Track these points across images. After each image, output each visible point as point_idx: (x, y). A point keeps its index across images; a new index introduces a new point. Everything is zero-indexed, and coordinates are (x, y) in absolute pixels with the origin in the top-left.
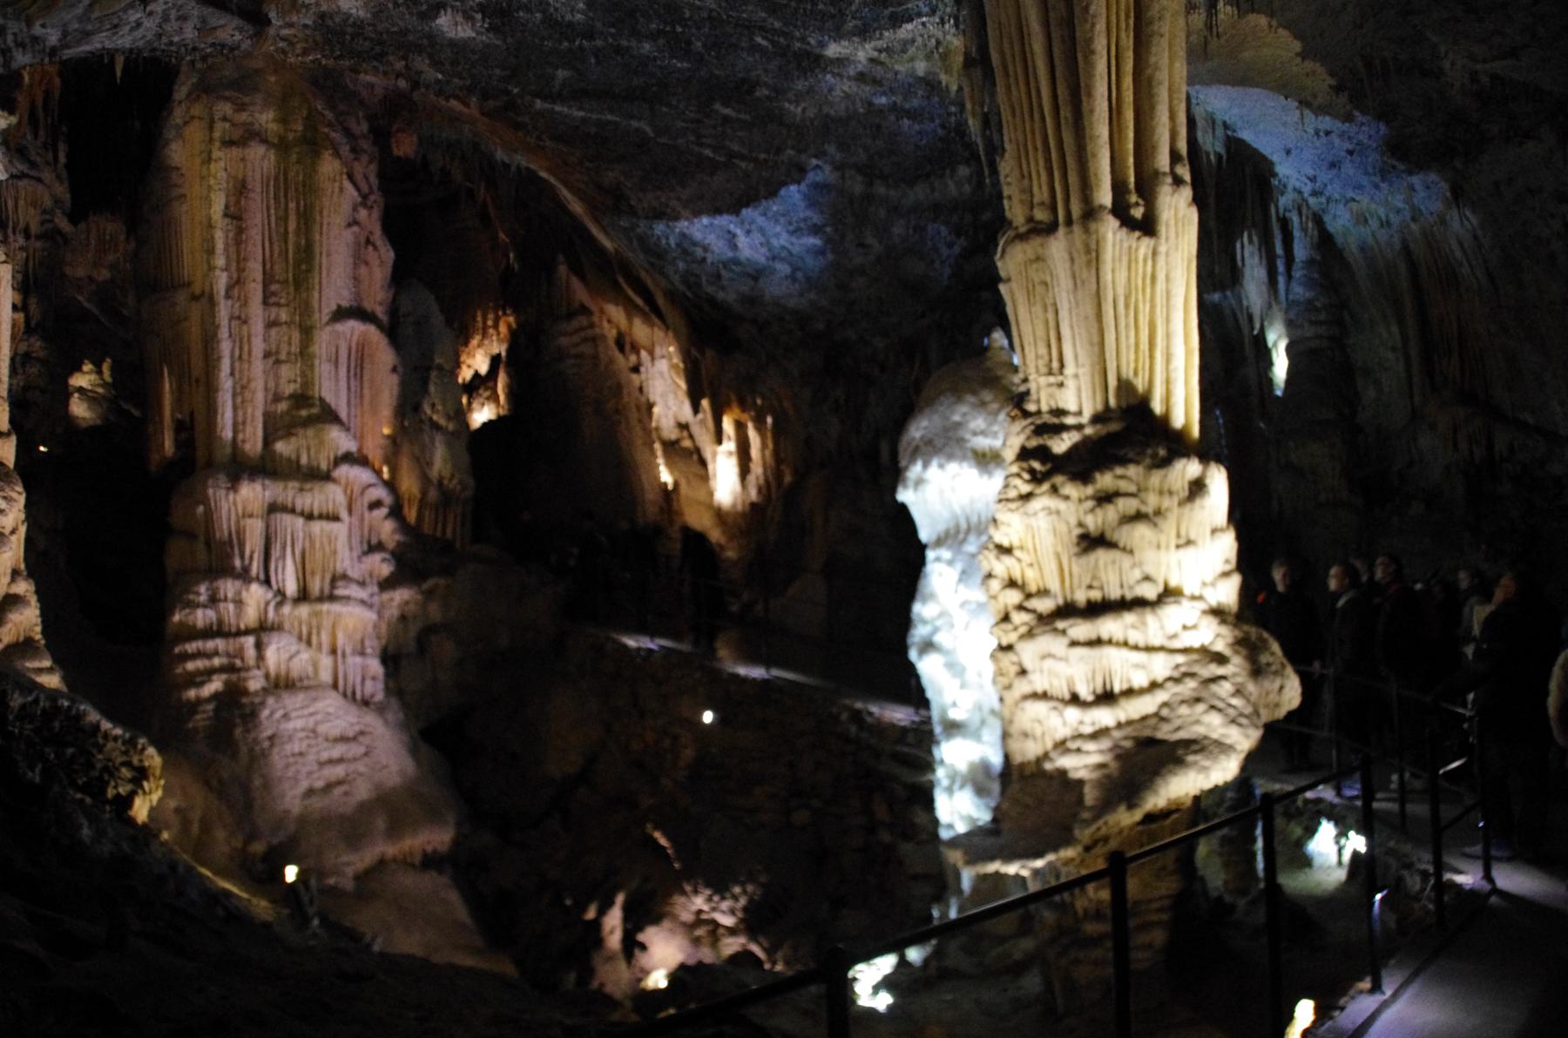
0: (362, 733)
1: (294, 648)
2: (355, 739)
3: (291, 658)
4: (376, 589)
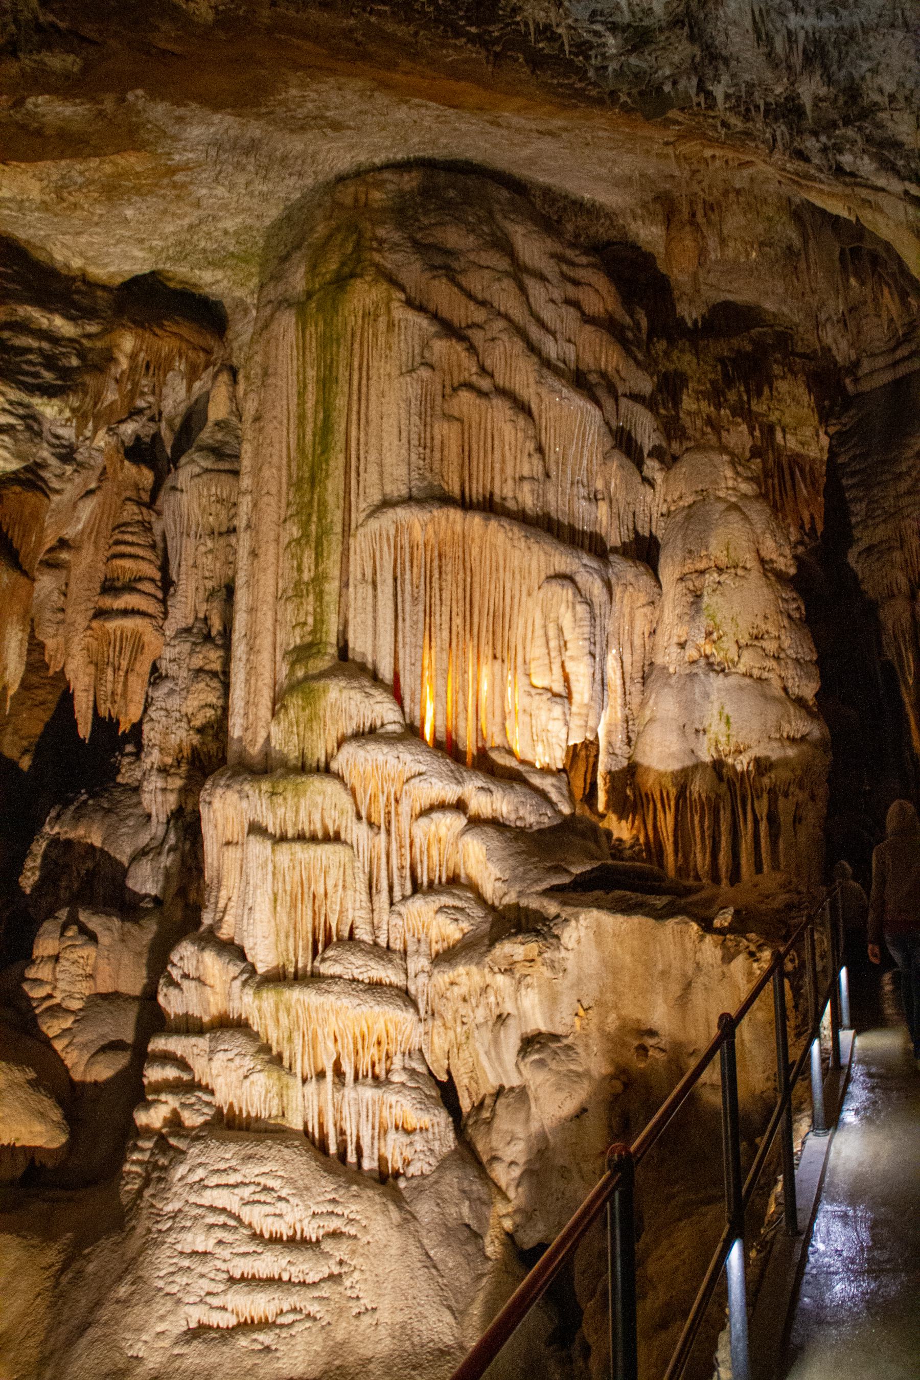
0: (335, 1235)
3: (246, 1077)
4: (424, 963)
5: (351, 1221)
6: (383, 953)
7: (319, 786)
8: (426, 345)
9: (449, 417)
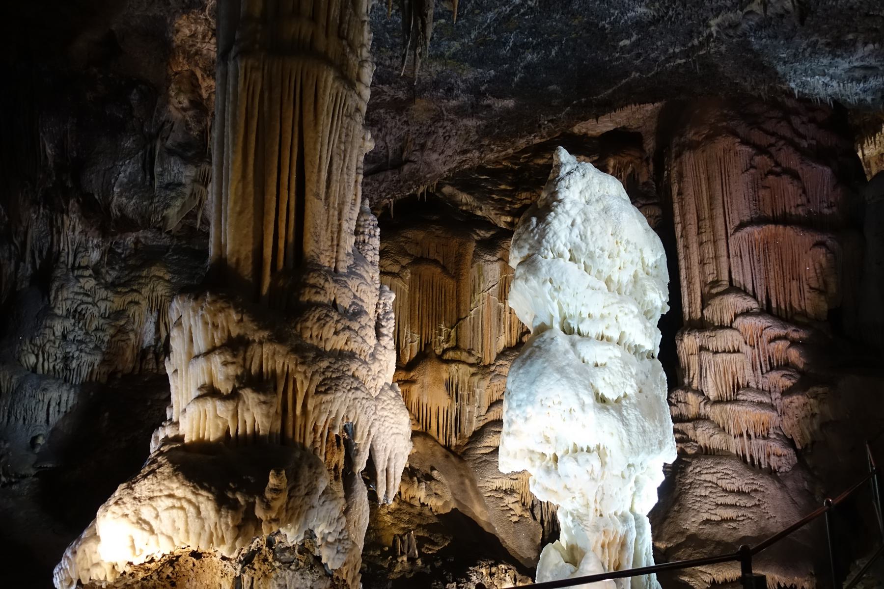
0: (756, 491)
1: (711, 431)
2: (749, 493)
4: (778, 395)
5: (760, 486)
6: (762, 391)
7: (728, 332)
8: (751, 159)
9: (765, 187)
